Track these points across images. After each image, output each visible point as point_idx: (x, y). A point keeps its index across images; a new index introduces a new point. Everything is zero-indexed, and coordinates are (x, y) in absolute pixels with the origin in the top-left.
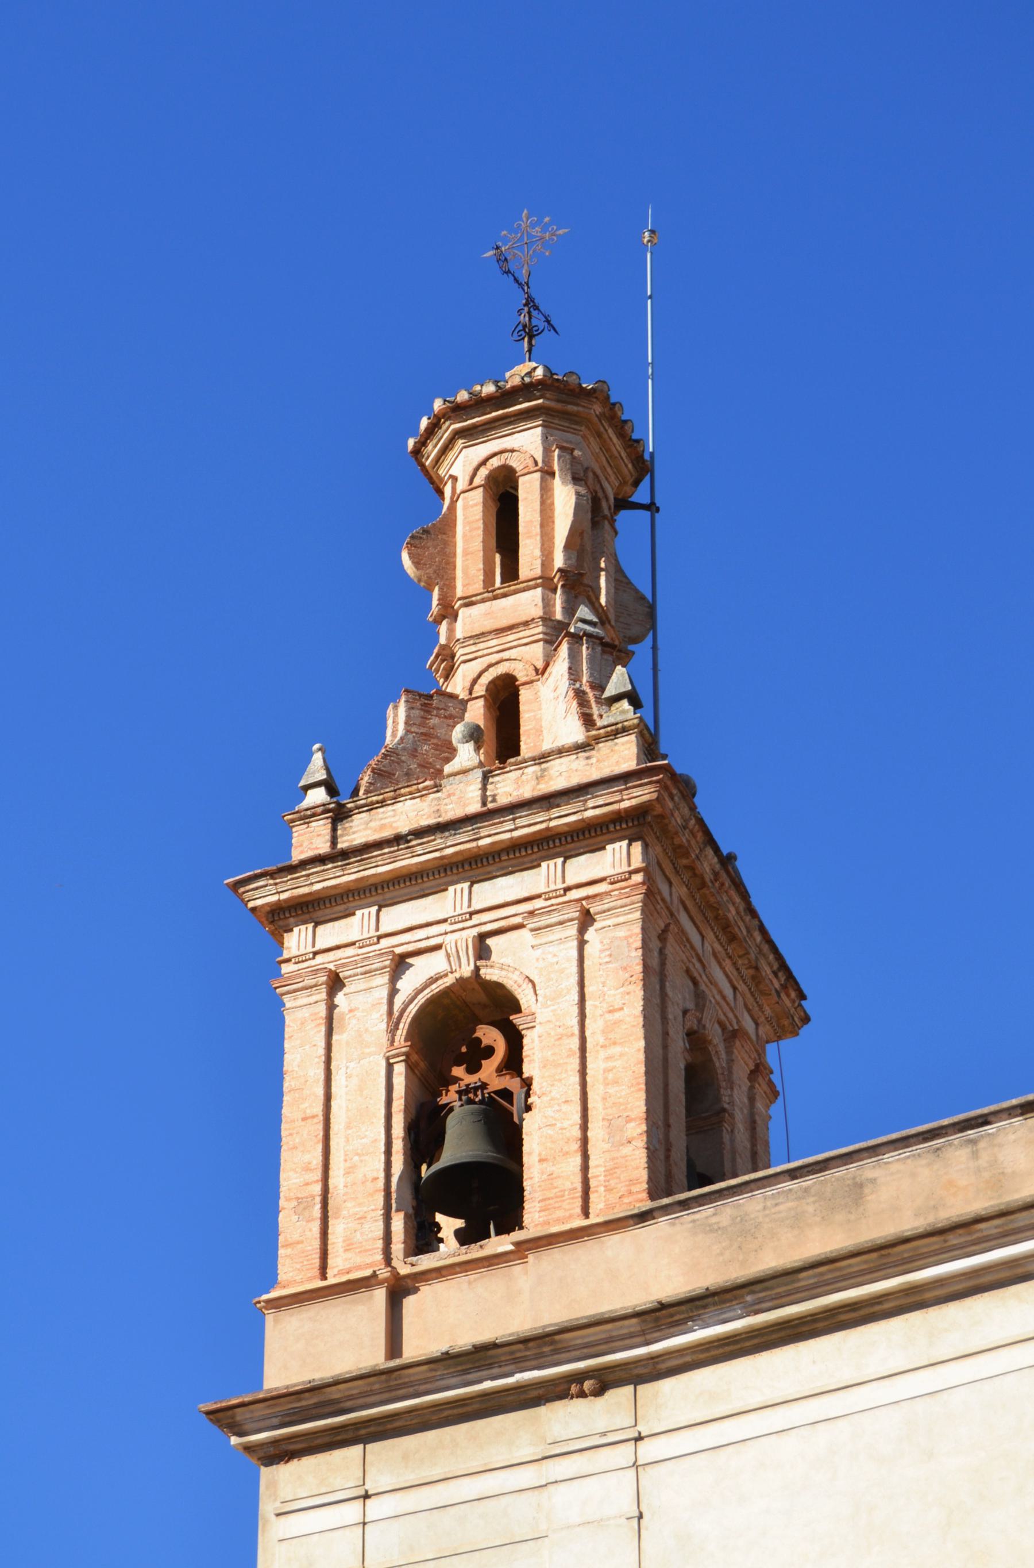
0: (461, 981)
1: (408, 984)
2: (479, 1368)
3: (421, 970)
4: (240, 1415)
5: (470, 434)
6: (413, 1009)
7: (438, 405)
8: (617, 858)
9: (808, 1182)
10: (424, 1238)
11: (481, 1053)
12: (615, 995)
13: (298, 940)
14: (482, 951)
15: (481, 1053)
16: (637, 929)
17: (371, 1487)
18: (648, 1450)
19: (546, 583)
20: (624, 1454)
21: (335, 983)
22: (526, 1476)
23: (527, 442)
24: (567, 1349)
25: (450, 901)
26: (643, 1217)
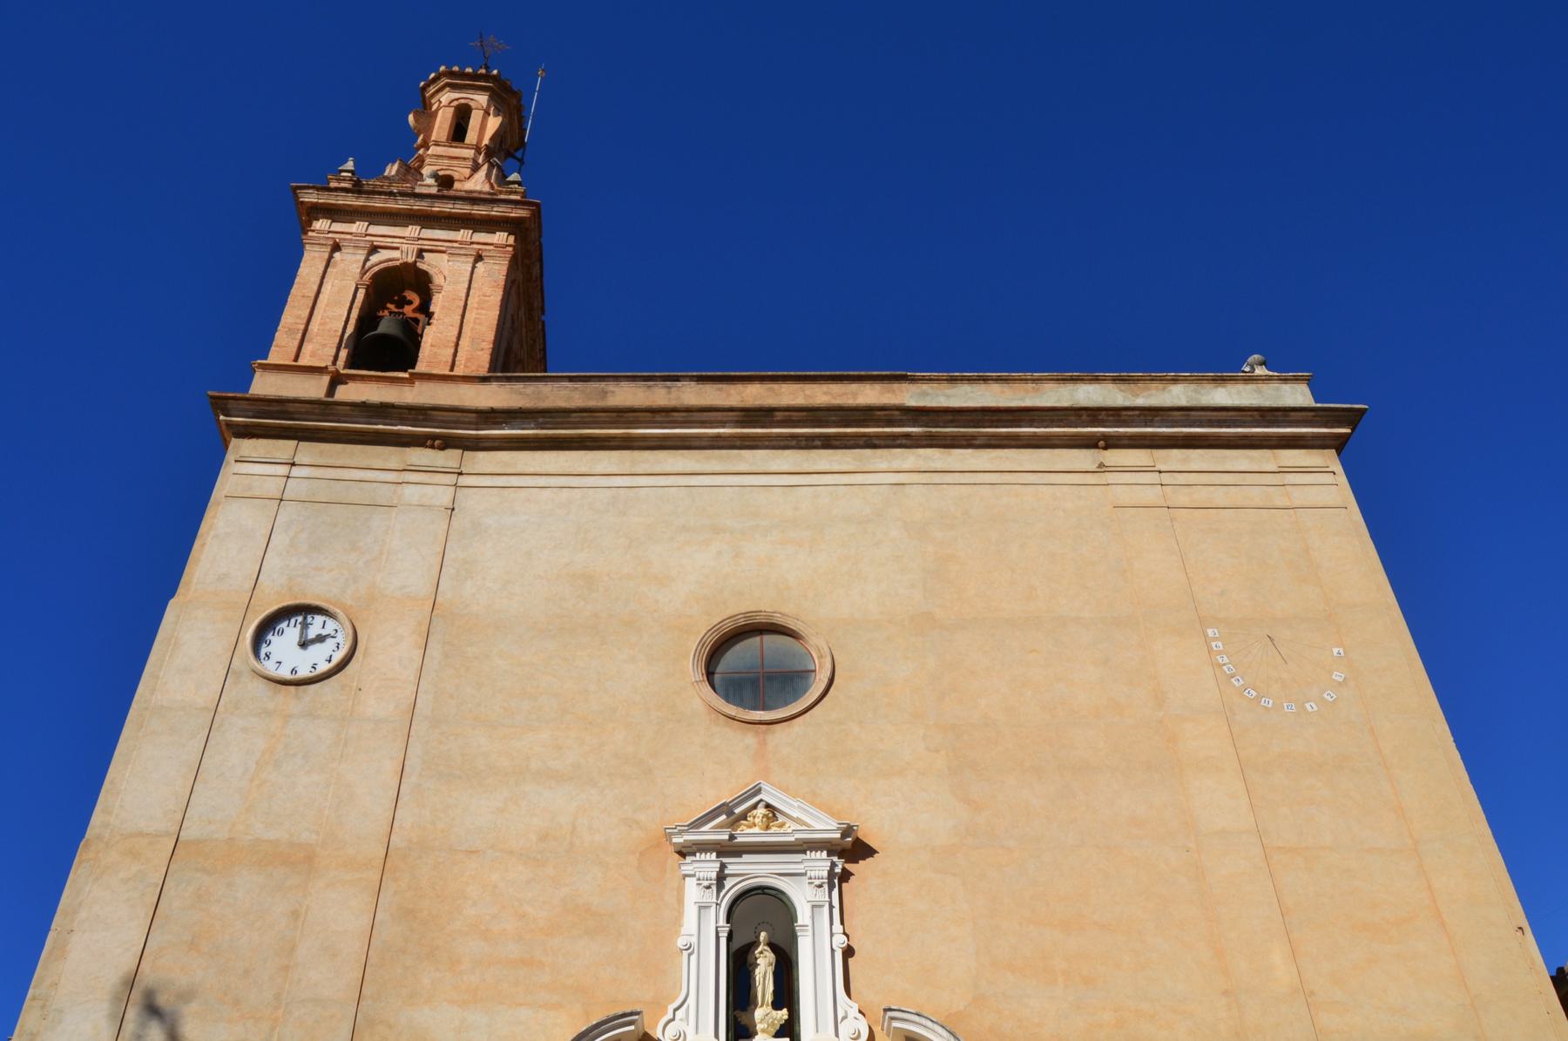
0: (406, 264)
1: (374, 259)
2: (378, 417)
3: (383, 255)
4: (231, 404)
5: (454, 87)
6: (376, 269)
7: (442, 68)
8: (500, 237)
9: (579, 385)
10: (352, 363)
11: (403, 302)
12: (487, 290)
13: (321, 224)
14: (420, 253)
15: (403, 302)
16: (505, 268)
18: (463, 480)
19: (478, 149)
20: (451, 479)
21: (336, 247)
23: (481, 99)
24: (433, 420)
25: (412, 231)
26: (484, 380)
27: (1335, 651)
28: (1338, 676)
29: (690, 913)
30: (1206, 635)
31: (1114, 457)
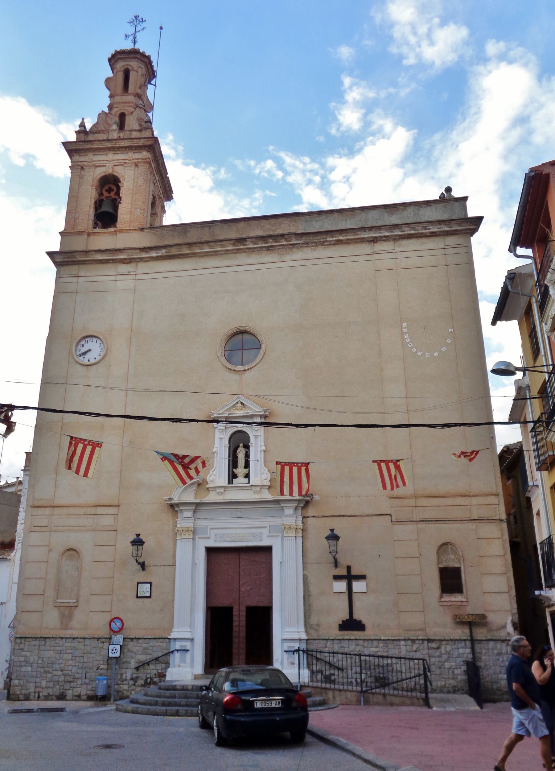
17: (80, 275)
18: (138, 277)
20: (132, 277)
22: (113, 278)
27: (450, 330)
28: (449, 341)
29: (217, 441)
30: (402, 326)
31: (379, 247)
